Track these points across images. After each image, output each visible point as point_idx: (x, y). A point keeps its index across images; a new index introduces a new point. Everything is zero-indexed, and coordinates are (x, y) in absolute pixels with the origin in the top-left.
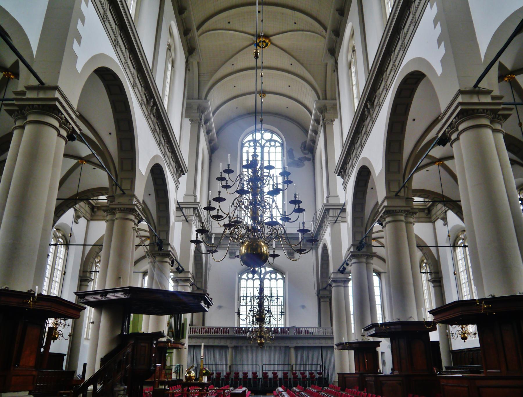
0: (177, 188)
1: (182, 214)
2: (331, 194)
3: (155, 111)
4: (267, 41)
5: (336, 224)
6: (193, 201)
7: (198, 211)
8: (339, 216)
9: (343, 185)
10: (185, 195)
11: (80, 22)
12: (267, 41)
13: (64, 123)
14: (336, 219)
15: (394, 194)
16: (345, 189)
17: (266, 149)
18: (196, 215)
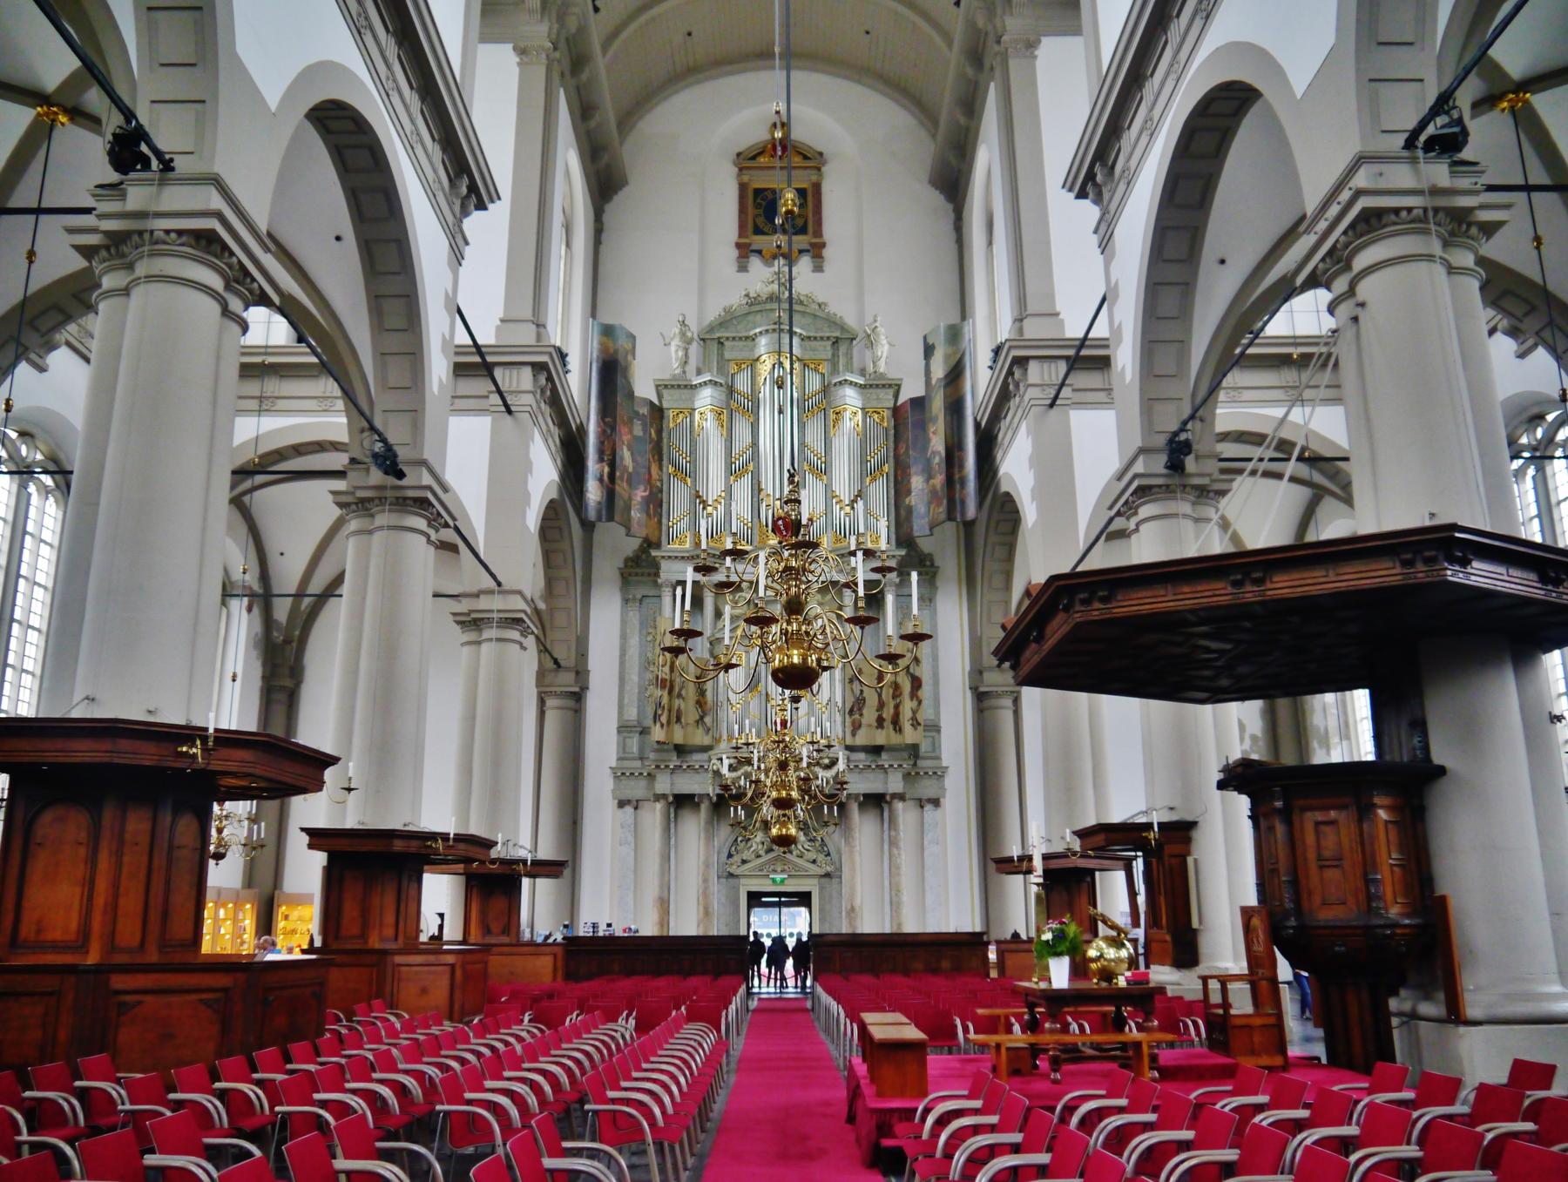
0: (457, 257)
1: (494, 389)
2: (1032, 307)
6: (533, 342)
7: (550, 379)
8: (1062, 385)
9: (1096, 232)
10: (502, 321)
14: (1053, 393)
15: (1400, 140)
16: (1106, 244)
18: (543, 391)
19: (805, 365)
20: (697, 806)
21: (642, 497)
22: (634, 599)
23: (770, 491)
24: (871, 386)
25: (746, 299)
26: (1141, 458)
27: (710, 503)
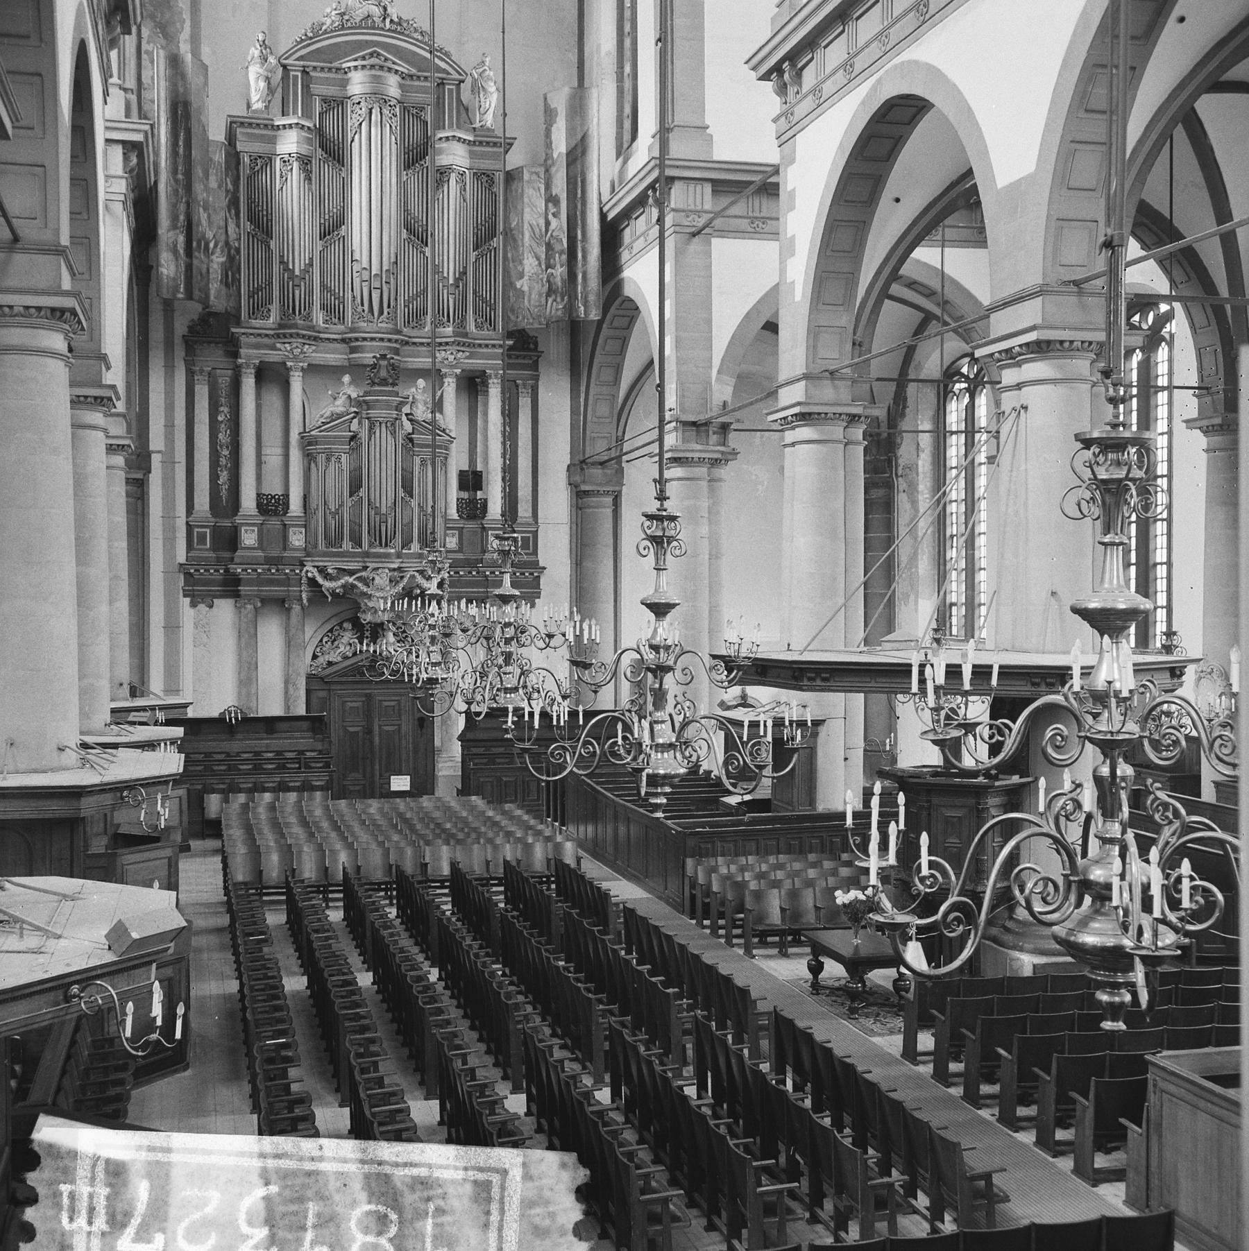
5: (696, 239)
9: (775, 120)
19: (405, 108)
20: (289, 610)
21: (222, 263)
22: (202, 371)
23: (365, 264)
24: (481, 143)
25: (339, 17)
26: (803, 383)
27: (297, 272)
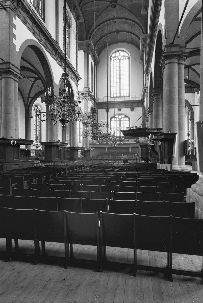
0: (77, 86)
3: (59, 56)
4: (116, 3)
7: (90, 94)
11: (14, 29)
12: (116, 3)
13: (15, 76)
17: (121, 61)
